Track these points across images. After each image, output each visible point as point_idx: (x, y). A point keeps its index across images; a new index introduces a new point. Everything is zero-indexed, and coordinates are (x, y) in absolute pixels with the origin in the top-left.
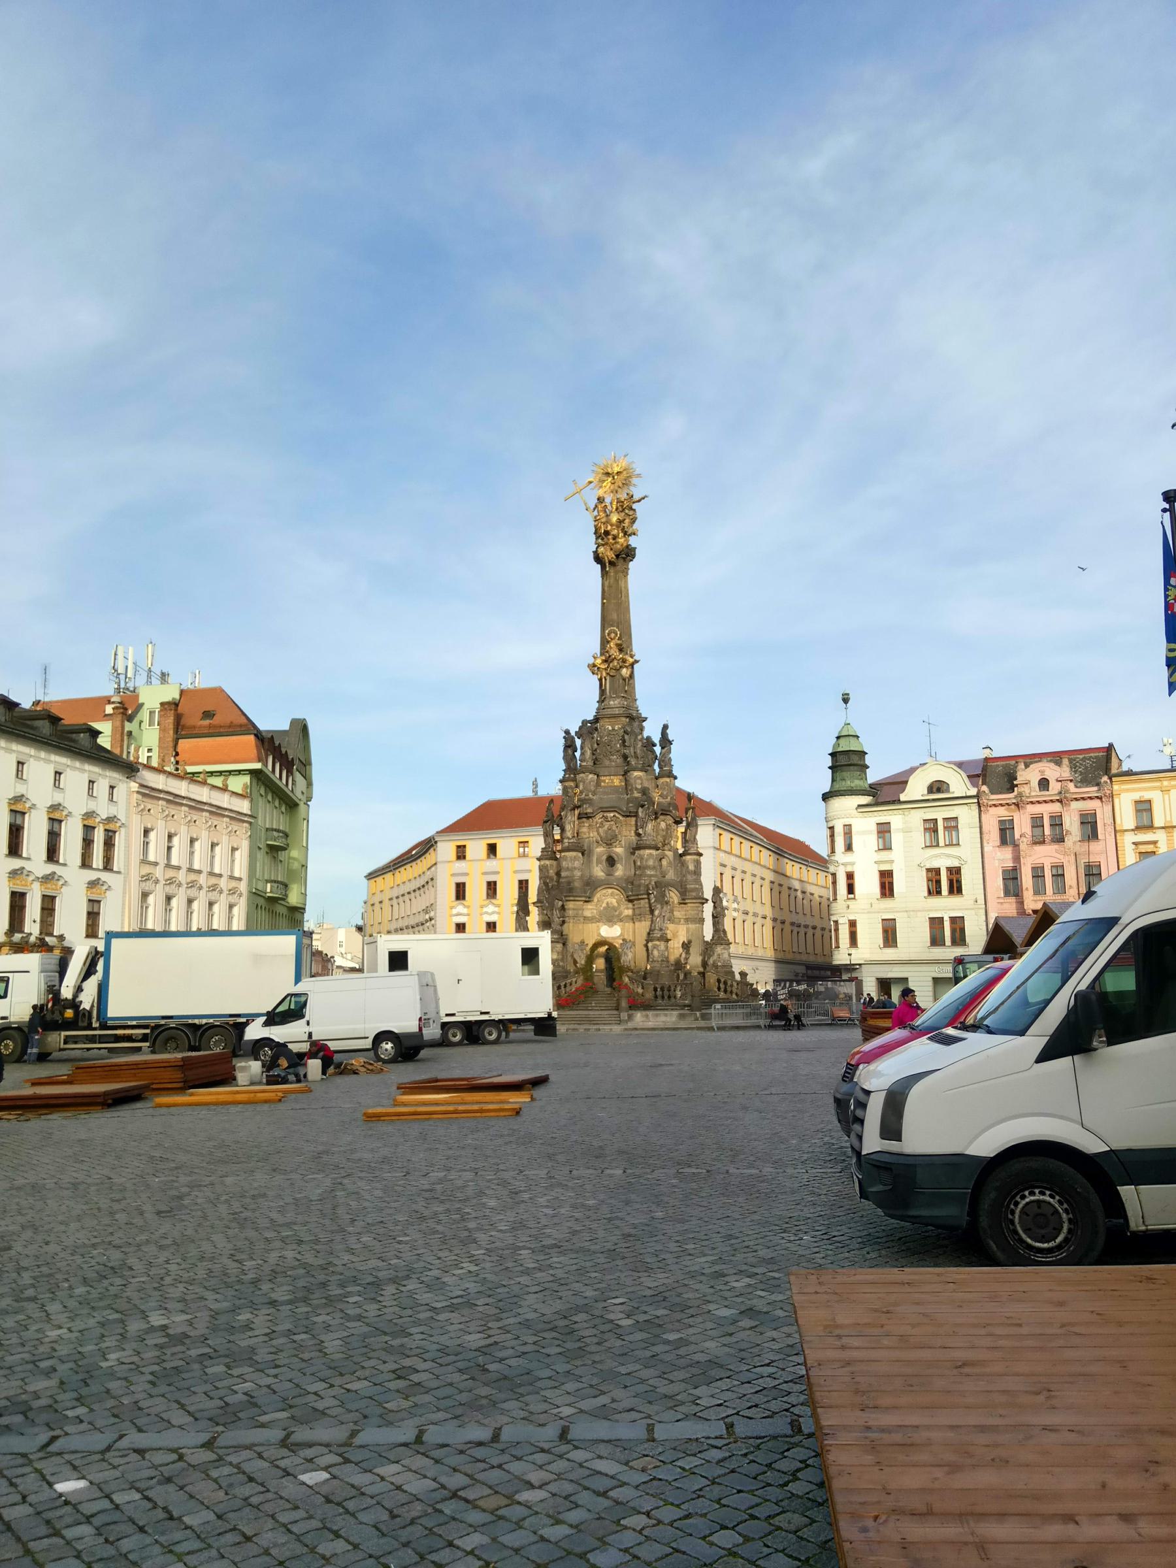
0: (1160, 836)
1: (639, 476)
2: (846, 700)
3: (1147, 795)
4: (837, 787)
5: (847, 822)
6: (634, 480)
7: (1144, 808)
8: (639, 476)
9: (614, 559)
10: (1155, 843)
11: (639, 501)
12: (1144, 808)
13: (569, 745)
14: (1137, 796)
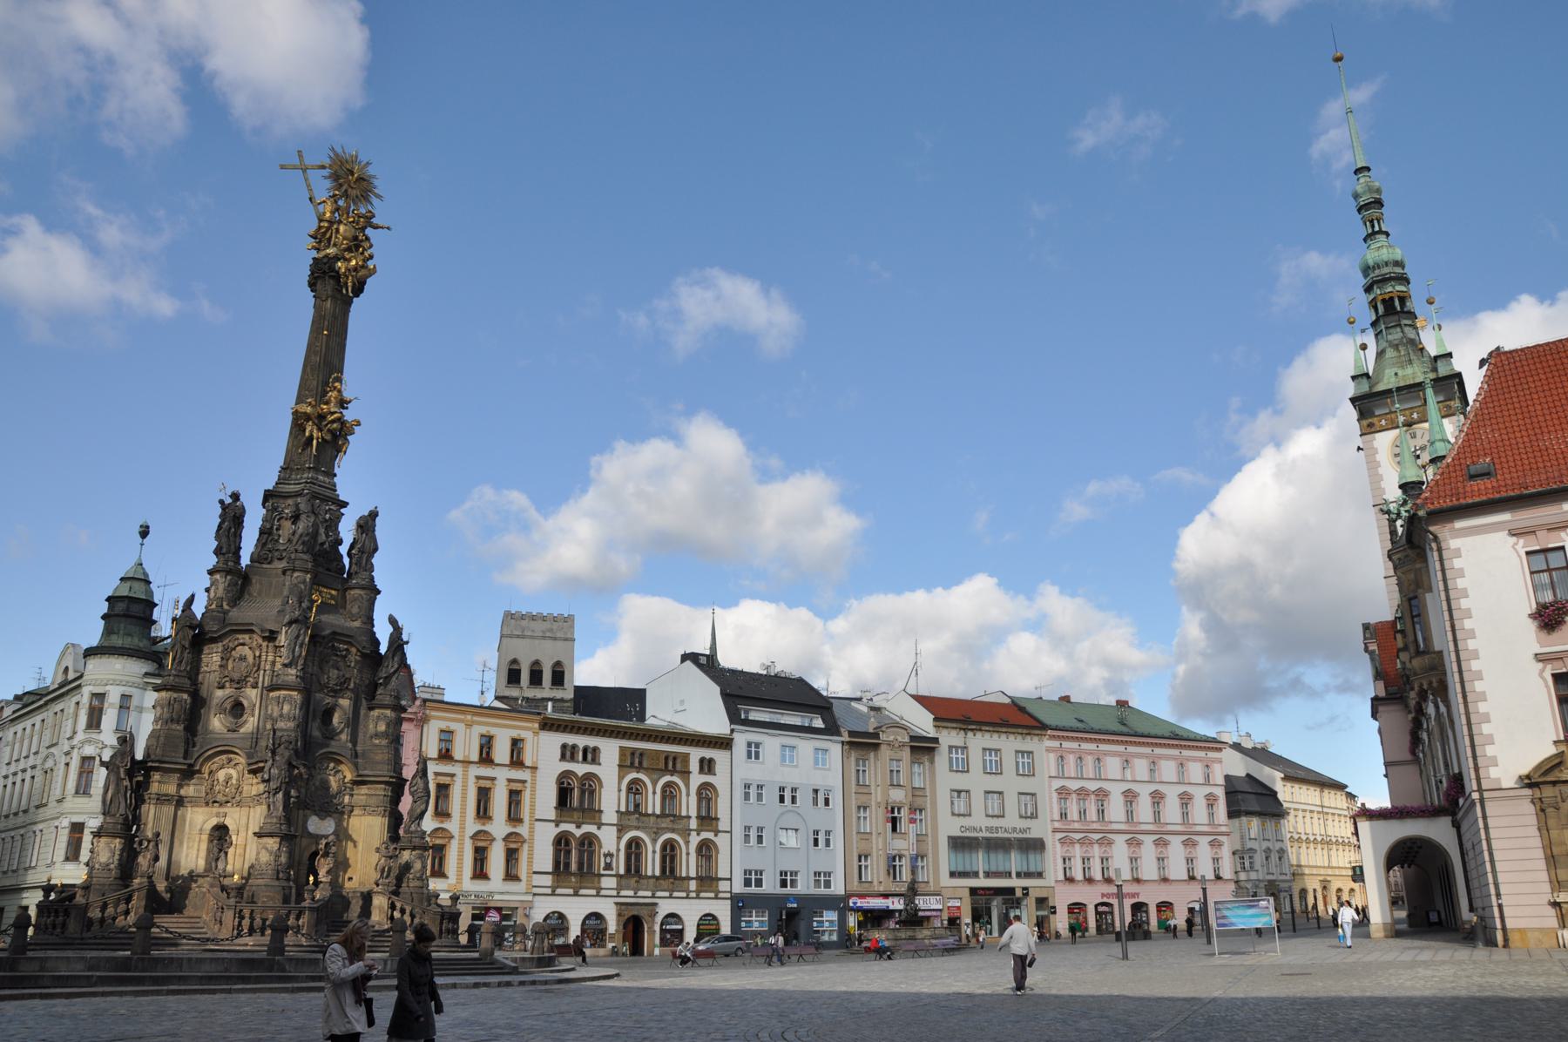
0: (456, 769)
1: (379, 196)
2: (144, 532)
3: (453, 726)
4: (117, 641)
5: (128, 690)
6: (374, 200)
7: (447, 736)
8: (379, 196)
9: (336, 283)
10: (453, 775)
11: (376, 227)
12: (447, 736)
13: (232, 516)
14: (444, 725)
